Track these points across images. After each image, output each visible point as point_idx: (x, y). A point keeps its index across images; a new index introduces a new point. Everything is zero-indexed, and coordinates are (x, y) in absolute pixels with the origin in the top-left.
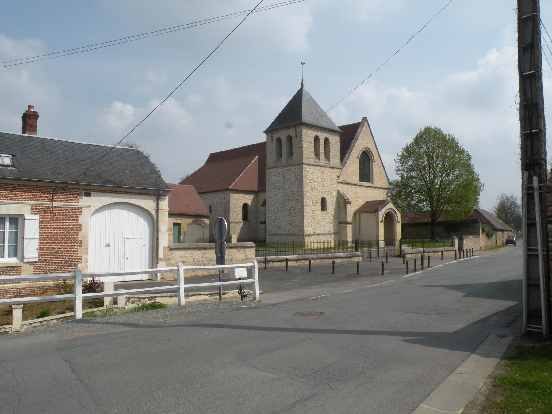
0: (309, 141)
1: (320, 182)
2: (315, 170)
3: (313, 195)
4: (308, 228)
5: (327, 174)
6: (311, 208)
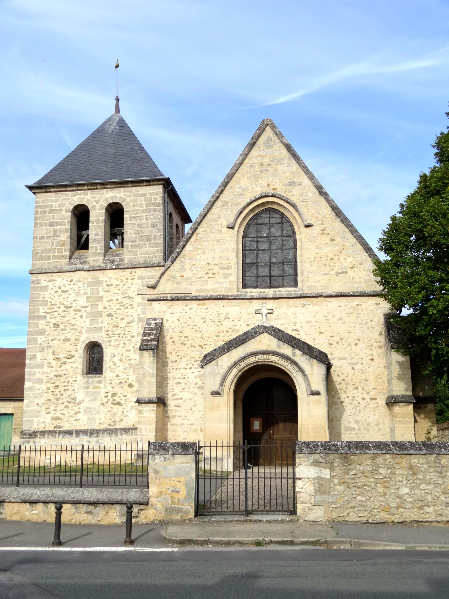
0: (55, 221)
1: (83, 307)
2: (69, 283)
3: (59, 340)
4: (37, 417)
5: (111, 285)
6: (45, 369)
